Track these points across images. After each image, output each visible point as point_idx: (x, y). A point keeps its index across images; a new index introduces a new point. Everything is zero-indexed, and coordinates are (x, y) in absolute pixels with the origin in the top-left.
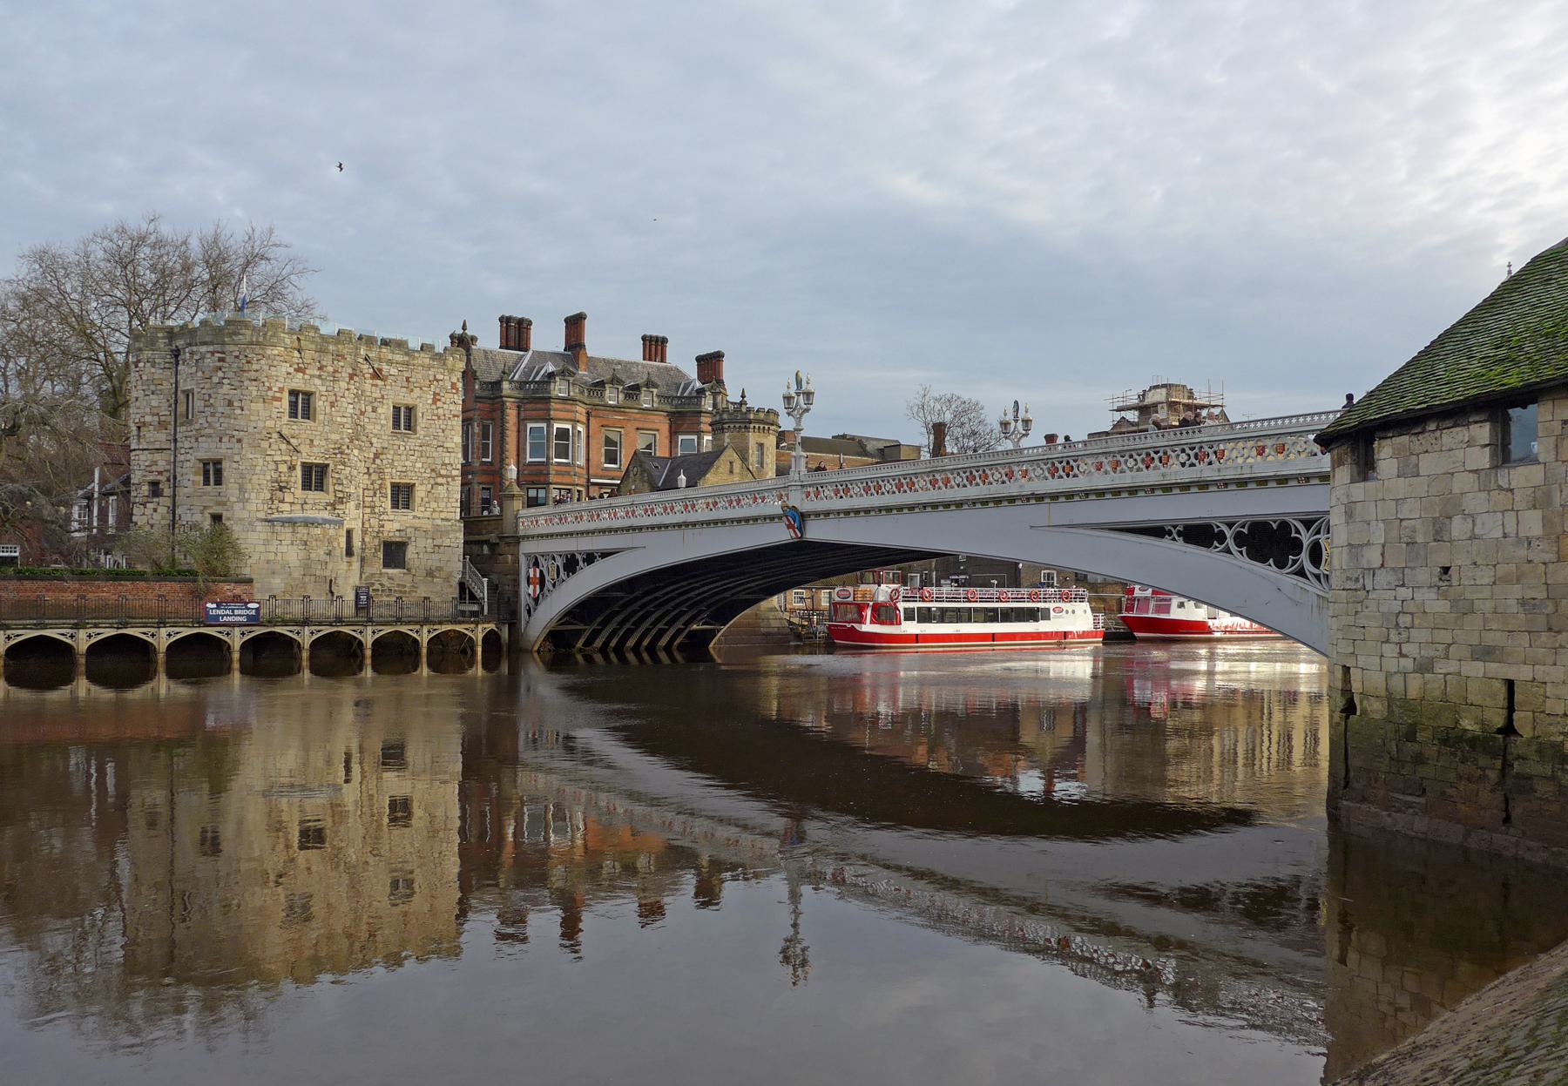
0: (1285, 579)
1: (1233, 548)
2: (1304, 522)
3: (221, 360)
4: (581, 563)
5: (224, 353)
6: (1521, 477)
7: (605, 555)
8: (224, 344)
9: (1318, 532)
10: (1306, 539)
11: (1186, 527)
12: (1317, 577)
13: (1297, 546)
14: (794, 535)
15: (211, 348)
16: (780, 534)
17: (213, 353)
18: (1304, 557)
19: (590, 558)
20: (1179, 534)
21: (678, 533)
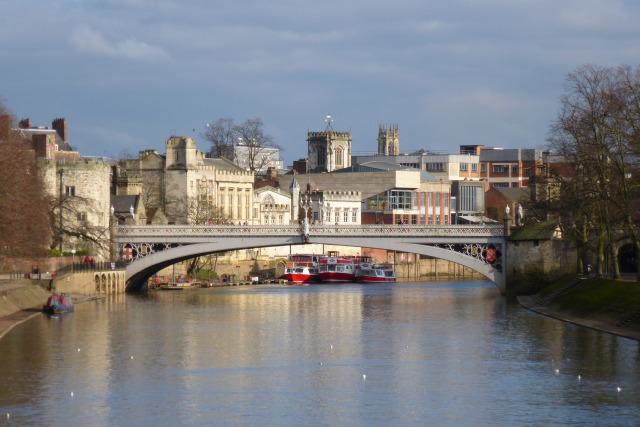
6: (537, 247)
7: (184, 244)
19: (174, 245)
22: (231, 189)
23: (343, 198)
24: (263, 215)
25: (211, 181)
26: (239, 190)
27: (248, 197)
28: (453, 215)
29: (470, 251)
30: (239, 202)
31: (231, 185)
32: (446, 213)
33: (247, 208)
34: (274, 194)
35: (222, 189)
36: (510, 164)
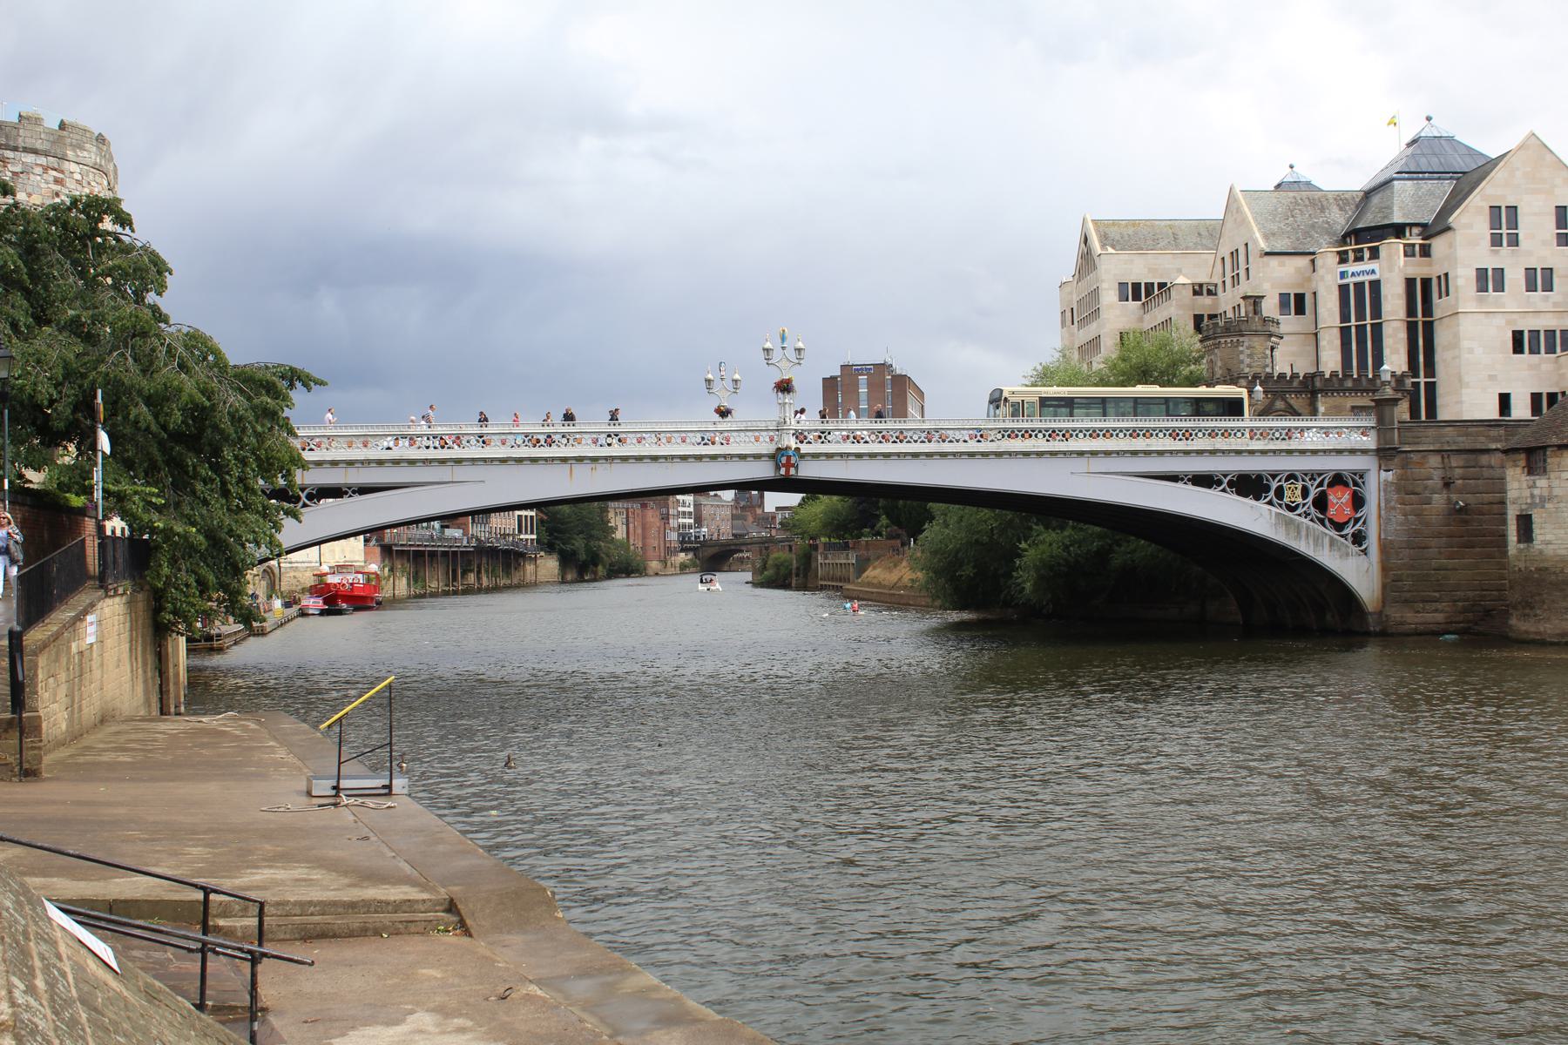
0: (1261, 505)
1: (1228, 489)
2: (1271, 475)
3: (57, 181)
4: (304, 499)
5: (62, 172)
8: (63, 158)
9: (1280, 481)
10: (1274, 485)
11: (1194, 476)
12: (1280, 505)
13: (1267, 489)
14: (783, 471)
15: (42, 160)
16: (764, 471)
17: (46, 169)
18: (1272, 494)
20: (1189, 480)
21: (567, 467)
29: (1280, 493)
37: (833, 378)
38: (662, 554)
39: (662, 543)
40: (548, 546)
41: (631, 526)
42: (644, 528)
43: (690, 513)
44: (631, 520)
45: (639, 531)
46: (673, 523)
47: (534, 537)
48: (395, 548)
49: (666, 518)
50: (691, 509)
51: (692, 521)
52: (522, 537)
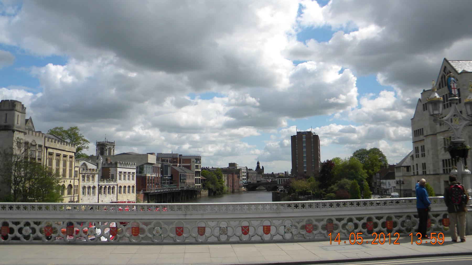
22: (58, 155)
23: (127, 167)
24: (81, 175)
25: (40, 146)
26: (65, 156)
27: (71, 163)
28: (161, 177)
30: (65, 165)
31: (59, 152)
32: (160, 176)
33: (71, 170)
34: (87, 163)
35: (51, 154)
36: (169, 159)
37: (294, 136)
38: (238, 188)
39: (238, 184)
40: (204, 186)
41: (229, 180)
42: (233, 180)
43: (246, 175)
44: (229, 178)
45: (231, 181)
46: (241, 178)
47: (200, 185)
48: (149, 194)
49: (239, 177)
50: (246, 174)
51: (246, 177)
52: (196, 185)
